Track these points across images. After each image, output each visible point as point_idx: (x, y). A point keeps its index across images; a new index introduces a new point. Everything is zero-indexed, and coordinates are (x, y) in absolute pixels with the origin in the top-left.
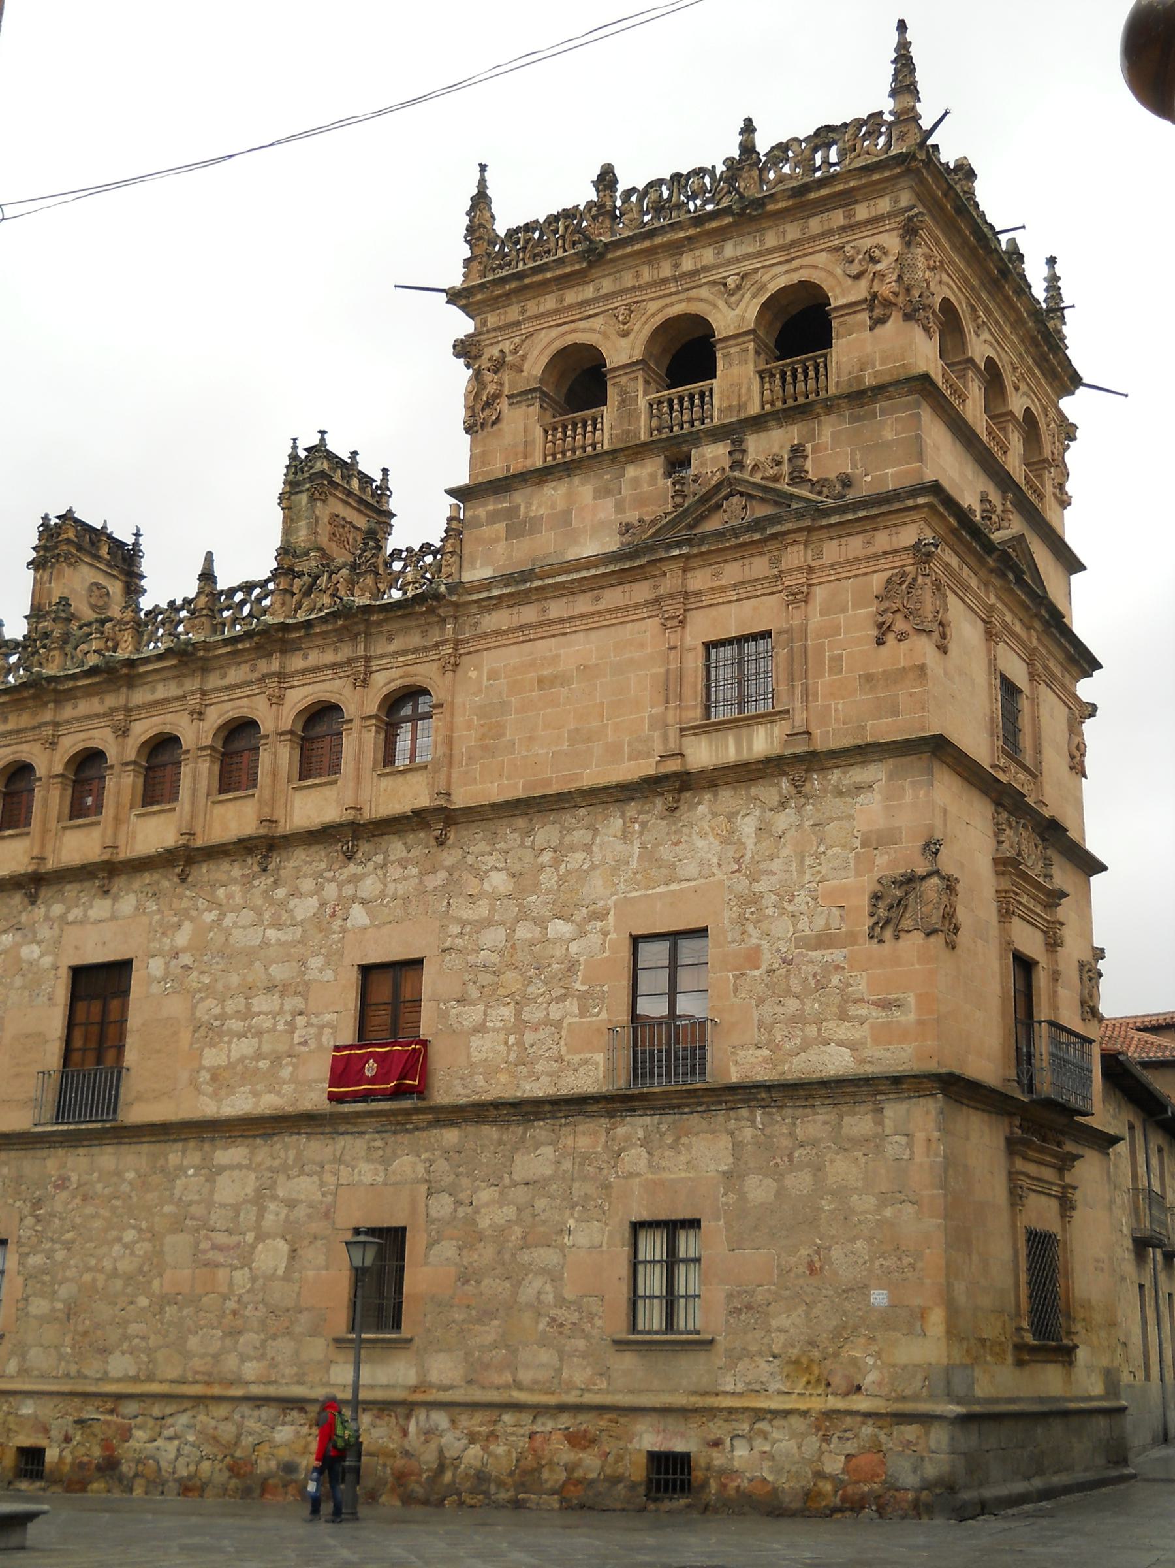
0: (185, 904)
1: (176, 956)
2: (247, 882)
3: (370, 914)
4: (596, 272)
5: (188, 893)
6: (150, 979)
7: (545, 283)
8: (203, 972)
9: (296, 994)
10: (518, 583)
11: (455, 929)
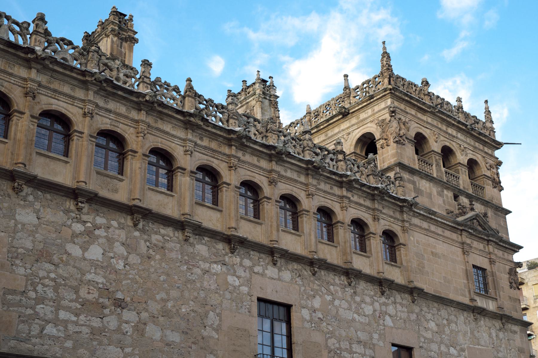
0: (316, 287)
1: (315, 311)
2: (343, 287)
3: (393, 322)
4: (429, 114)
5: (316, 282)
6: (303, 320)
7: (414, 105)
8: (329, 324)
9: (370, 348)
10: (430, 214)
11: (423, 340)
